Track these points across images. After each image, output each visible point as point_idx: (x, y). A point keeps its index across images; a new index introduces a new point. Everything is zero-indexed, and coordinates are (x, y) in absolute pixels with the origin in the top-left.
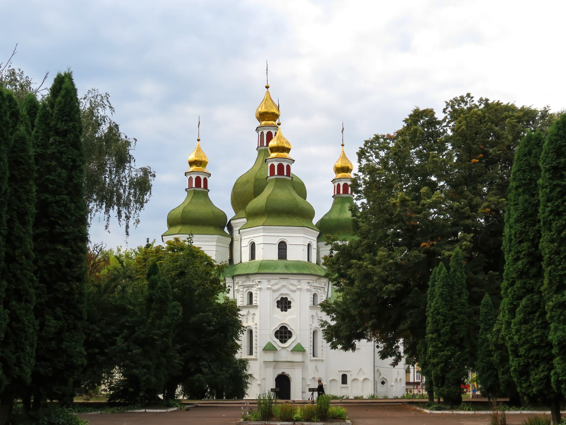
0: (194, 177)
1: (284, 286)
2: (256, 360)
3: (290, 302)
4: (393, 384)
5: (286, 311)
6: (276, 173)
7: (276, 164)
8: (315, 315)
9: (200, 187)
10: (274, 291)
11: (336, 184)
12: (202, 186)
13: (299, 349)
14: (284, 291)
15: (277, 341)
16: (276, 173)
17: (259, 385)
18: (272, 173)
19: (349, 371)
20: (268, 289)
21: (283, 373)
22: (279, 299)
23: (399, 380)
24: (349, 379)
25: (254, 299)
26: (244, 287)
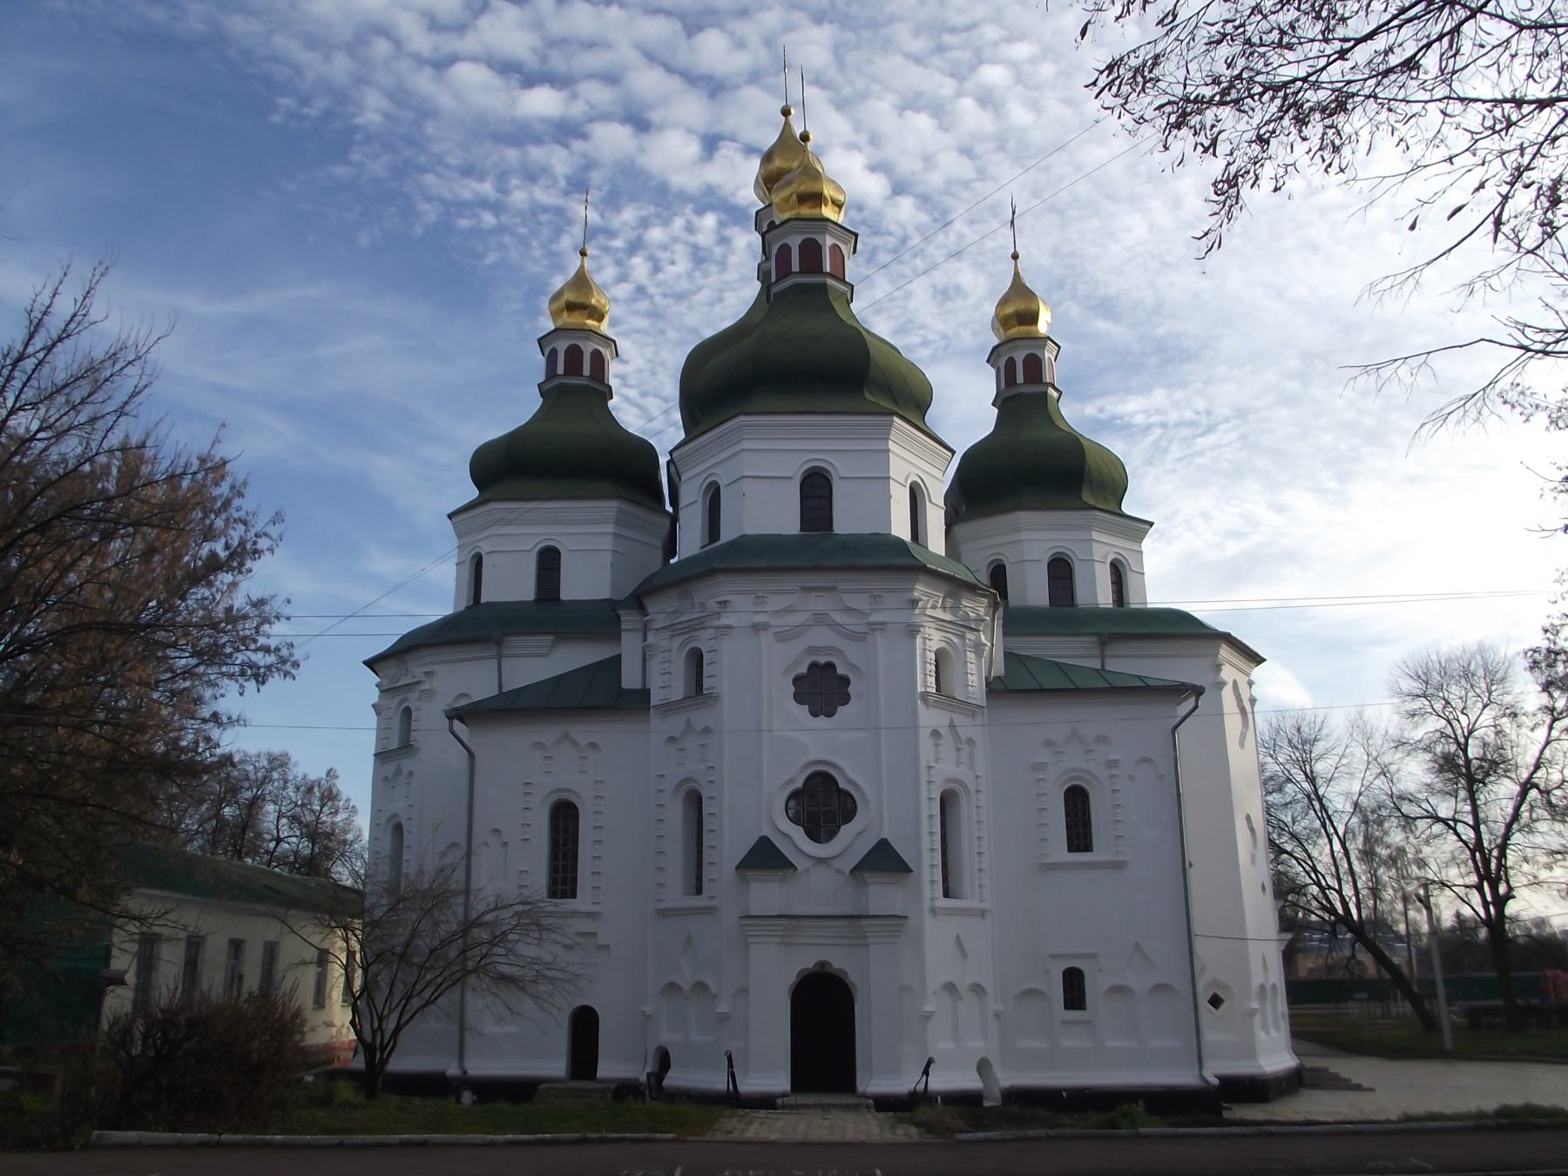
0: (562, 346)
1: (820, 619)
2: (709, 910)
3: (845, 681)
4: (1255, 1005)
5: (830, 714)
6: (795, 267)
7: (795, 242)
8: (943, 731)
9: (579, 373)
10: (783, 637)
11: (1002, 363)
12: (586, 371)
13: (884, 861)
14: (821, 637)
15: (798, 833)
16: (795, 267)
17: (723, 1018)
18: (784, 270)
19: (1093, 956)
20: (757, 628)
21: (822, 964)
22: (803, 669)
23: (1268, 987)
24: (1094, 988)
25: (706, 670)
26: (672, 629)
